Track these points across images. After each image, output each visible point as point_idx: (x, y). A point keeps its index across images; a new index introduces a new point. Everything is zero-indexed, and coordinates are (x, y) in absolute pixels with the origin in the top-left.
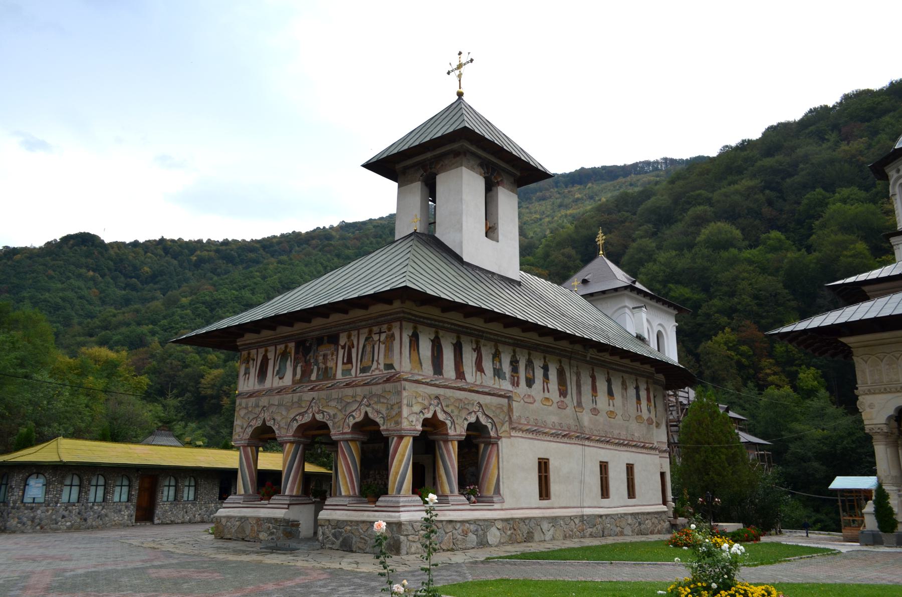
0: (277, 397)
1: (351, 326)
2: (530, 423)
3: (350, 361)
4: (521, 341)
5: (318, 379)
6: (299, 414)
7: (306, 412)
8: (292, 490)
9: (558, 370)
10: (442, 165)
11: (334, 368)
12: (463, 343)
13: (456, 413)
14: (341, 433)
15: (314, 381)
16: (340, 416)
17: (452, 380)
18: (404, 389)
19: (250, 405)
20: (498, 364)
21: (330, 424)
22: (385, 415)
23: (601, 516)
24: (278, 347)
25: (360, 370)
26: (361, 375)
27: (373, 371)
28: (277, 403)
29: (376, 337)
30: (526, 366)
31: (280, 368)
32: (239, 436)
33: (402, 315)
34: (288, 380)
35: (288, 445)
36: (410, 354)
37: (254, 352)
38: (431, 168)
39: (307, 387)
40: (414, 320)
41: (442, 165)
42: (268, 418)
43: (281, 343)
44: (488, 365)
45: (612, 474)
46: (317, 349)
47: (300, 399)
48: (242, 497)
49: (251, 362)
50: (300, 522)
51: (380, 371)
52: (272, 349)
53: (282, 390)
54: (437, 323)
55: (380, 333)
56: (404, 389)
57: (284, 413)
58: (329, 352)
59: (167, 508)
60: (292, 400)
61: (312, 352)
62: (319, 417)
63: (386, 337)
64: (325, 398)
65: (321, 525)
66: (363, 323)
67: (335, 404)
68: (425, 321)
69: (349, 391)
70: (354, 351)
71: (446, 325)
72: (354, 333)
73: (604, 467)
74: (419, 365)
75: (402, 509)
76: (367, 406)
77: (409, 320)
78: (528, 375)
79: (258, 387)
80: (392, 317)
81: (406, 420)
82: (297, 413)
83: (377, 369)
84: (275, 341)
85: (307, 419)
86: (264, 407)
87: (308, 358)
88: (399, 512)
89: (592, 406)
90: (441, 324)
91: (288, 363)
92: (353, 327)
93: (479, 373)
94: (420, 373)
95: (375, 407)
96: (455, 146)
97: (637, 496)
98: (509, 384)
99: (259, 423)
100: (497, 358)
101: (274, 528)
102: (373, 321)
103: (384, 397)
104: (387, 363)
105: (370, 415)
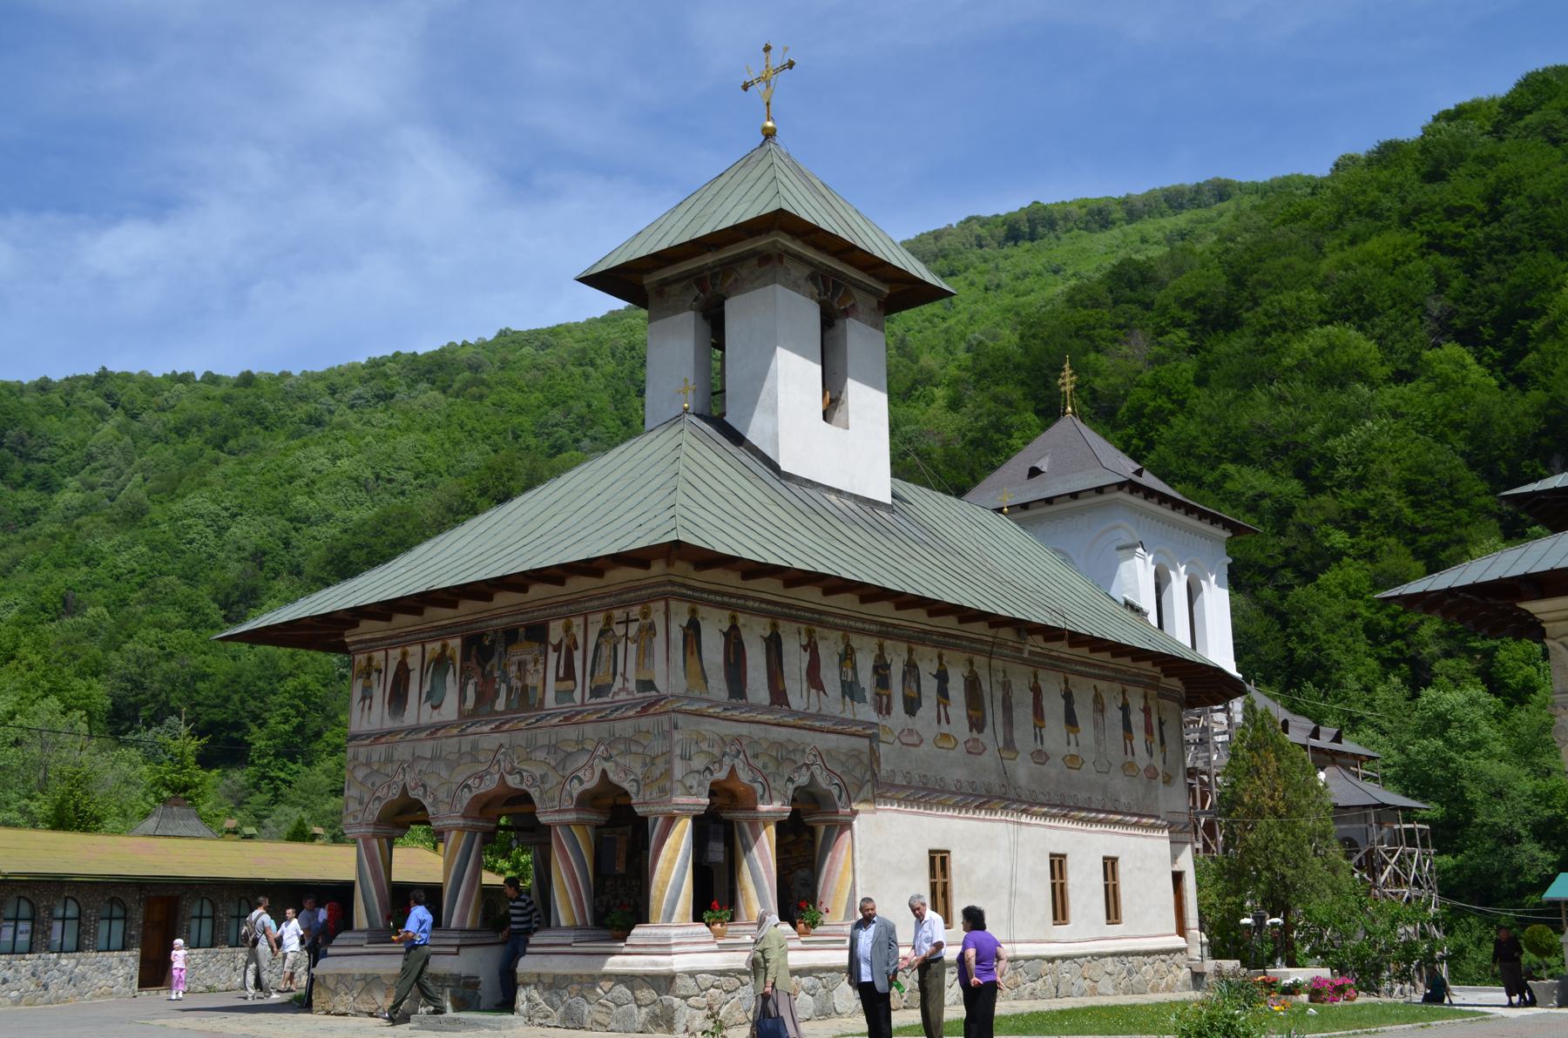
0: (430, 743)
1: (572, 608)
2: (914, 784)
3: (570, 674)
4: (894, 626)
5: (508, 710)
7: (487, 772)
8: (463, 918)
9: (966, 679)
10: (736, 280)
11: (540, 689)
12: (782, 635)
13: (772, 767)
15: (502, 713)
16: (554, 779)
17: (764, 707)
18: (676, 728)
19: (375, 758)
20: (850, 673)
21: (535, 793)
23: (1052, 960)
24: (429, 647)
26: (593, 701)
27: (615, 693)
28: (428, 755)
30: (904, 674)
31: (432, 687)
32: (355, 818)
33: (669, 588)
34: (450, 709)
35: (454, 833)
36: (685, 661)
37: (379, 656)
38: (714, 285)
39: (488, 723)
40: (690, 597)
41: (736, 280)
43: (433, 639)
44: (830, 674)
45: (1073, 879)
47: (475, 747)
48: (365, 935)
49: (374, 676)
50: (481, 979)
51: (629, 693)
52: (415, 650)
54: (733, 601)
55: (627, 621)
56: (676, 728)
57: (444, 774)
58: (529, 657)
59: (198, 961)
61: (497, 655)
62: (513, 781)
63: (640, 630)
64: (524, 744)
66: (596, 603)
67: (544, 755)
68: (712, 597)
69: (571, 733)
70: (578, 655)
71: (750, 603)
72: (577, 622)
73: (1057, 863)
74: (702, 682)
75: (675, 949)
77: (682, 598)
78: (907, 692)
79: (389, 724)
80: (650, 591)
81: (679, 785)
82: (468, 774)
83: (623, 689)
85: (490, 785)
86: (404, 762)
87: (488, 668)
88: (670, 954)
89: (1033, 746)
90: (741, 602)
91: (450, 677)
92: (575, 608)
93: (813, 691)
94: (704, 696)
95: (621, 760)
96: (761, 243)
97: (1124, 920)
98: (872, 708)
99: (395, 793)
100: (848, 662)
102: (612, 599)
104: (641, 678)
105: (613, 777)
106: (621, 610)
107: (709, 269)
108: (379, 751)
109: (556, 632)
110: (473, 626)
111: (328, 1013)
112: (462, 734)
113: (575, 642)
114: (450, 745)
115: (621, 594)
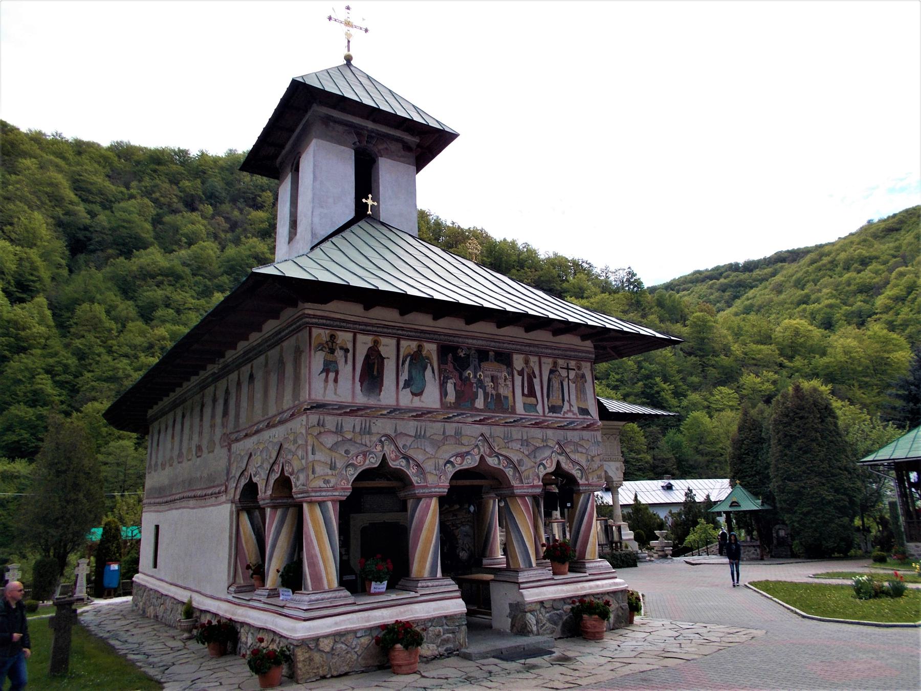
1: (532, 349)
3: (532, 393)
5: (487, 407)
6: (457, 455)
11: (511, 398)
14: (531, 486)
15: (481, 410)
16: (528, 463)
22: (586, 468)
24: (404, 343)
25: (549, 408)
26: (551, 414)
29: (564, 373)
32: (327, 482)
37: (344, 337)
39: (472, 416)
42: (393, 456)
46: (480, 366)
49: (339, 354)
51: (574, 414)
53: (424, 414)
60: (444, 433)
65: (531, 611)
66: (550, 351)
67: (519, 446)
69: (537, 433)
70: (536, 381)
76: (558, 453)
79: (361, 399)
80: (584, 354)
82: (453, 452)
83: (570, 411)
84: (400, 332)
85: (470, 462)
91: (428, 373)
101: (447, 631)
102: (560, 352)
103: (582, 446)
106: (563, 361)
107: (368, 131)
108: (349, 423)
109: (518, 361)
110: (456, 339)
111: (324, 677)
112: (447, 420)
113: (533, 372)
114: (435, 428)
115: (566, 351)
